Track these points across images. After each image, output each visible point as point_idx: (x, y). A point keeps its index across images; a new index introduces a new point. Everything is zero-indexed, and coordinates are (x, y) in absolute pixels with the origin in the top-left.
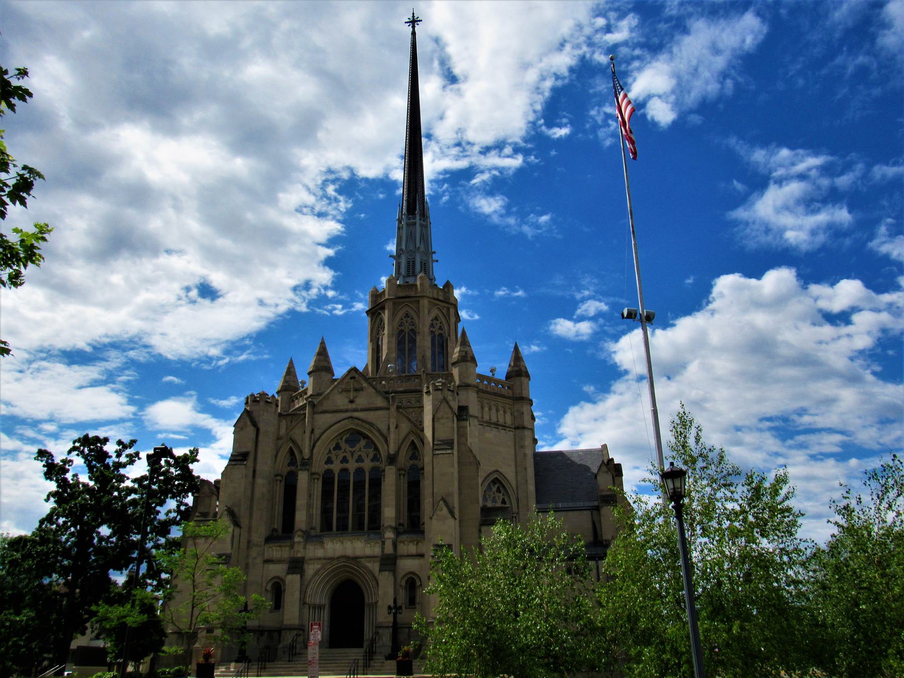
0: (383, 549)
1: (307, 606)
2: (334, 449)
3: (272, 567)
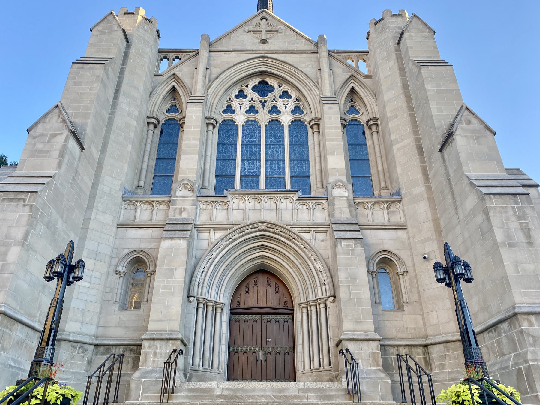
0: (331, 214)
2: (237, 96)
3: (132, 233)
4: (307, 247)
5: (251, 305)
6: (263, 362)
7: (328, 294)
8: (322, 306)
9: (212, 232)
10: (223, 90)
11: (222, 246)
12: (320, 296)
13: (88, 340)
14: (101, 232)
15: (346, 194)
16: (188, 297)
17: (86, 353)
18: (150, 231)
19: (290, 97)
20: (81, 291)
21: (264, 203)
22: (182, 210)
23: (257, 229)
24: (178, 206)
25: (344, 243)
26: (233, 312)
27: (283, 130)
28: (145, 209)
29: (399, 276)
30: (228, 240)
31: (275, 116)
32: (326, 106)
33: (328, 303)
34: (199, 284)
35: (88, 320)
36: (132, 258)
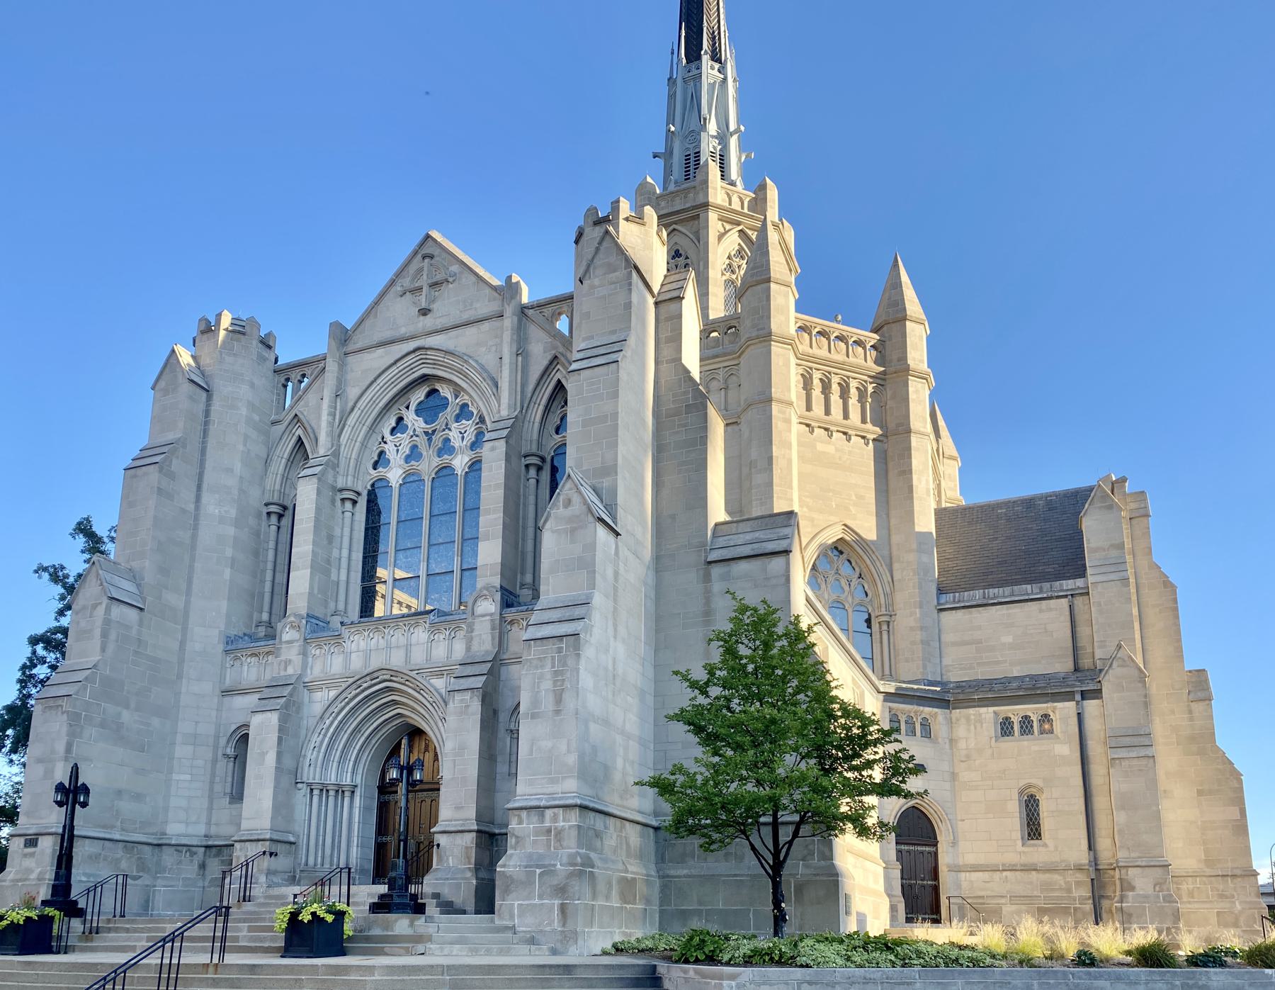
1: (304, 790)
2: (393, 431)
22: (288, 662)
24: (283, 658)
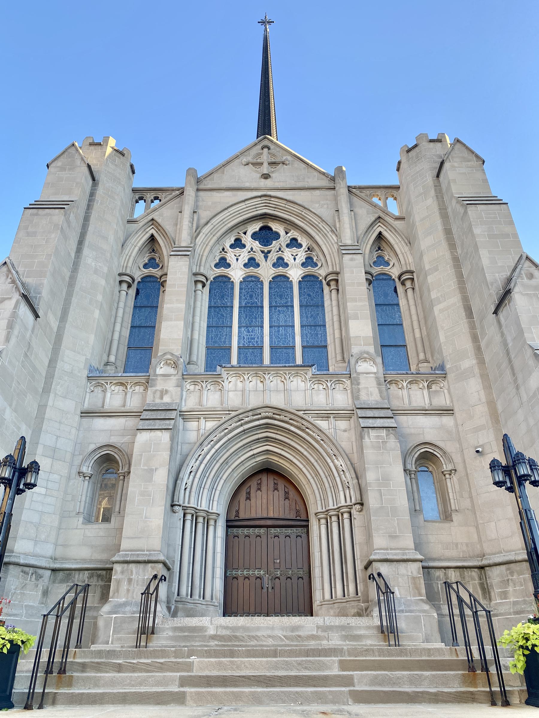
0: (355, 396)
2: (232, 246)
3: (100, 423)
4: (325, 439)
5: (253, 516)
6: (270, 590)
7: (353, 501)
8: (346, 516)
9: (202, 421)
10: (215, 238)
11: (215, 439)
12: (343, 503)
13: (43, 564)
14: (60, 423)
15: (374, 370)
16: (172, 506)
17: (41, 580)
18: (122, 420)
19: (300, 246)
20: (34, 499)
21: (267, 382)
22: (163, 393)
23: (260, 416)
24: (159, 387)
25: (373, 433)
26: (230, 525)
27: (292, 288)
28: (116, 391)
29: (445, 475)
30: (223, 431)
31: (281, 270)
32: (347, 257)
33: (353, 511)
34: (185, 489)
35: (43, 537)
36: (99, 455)
